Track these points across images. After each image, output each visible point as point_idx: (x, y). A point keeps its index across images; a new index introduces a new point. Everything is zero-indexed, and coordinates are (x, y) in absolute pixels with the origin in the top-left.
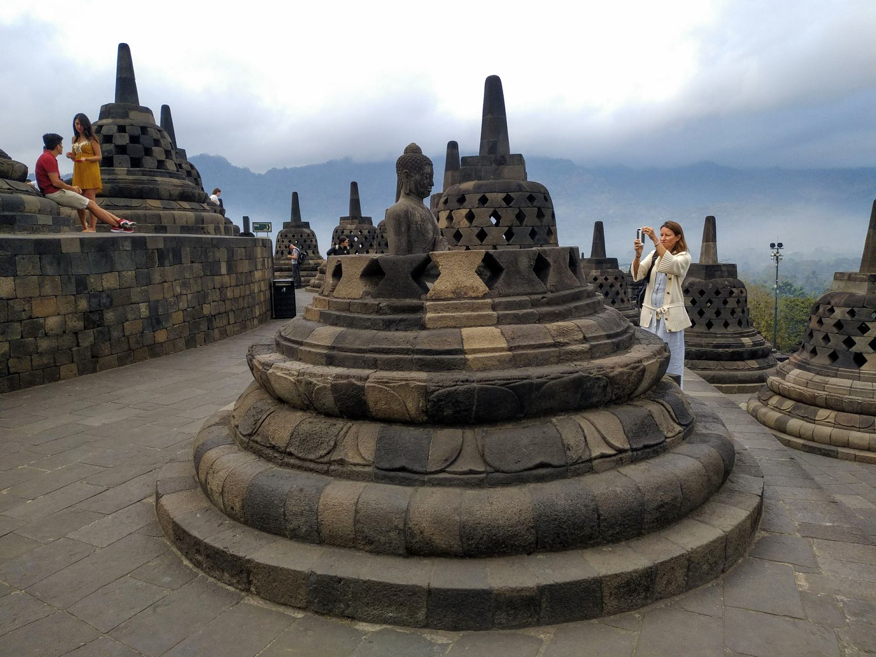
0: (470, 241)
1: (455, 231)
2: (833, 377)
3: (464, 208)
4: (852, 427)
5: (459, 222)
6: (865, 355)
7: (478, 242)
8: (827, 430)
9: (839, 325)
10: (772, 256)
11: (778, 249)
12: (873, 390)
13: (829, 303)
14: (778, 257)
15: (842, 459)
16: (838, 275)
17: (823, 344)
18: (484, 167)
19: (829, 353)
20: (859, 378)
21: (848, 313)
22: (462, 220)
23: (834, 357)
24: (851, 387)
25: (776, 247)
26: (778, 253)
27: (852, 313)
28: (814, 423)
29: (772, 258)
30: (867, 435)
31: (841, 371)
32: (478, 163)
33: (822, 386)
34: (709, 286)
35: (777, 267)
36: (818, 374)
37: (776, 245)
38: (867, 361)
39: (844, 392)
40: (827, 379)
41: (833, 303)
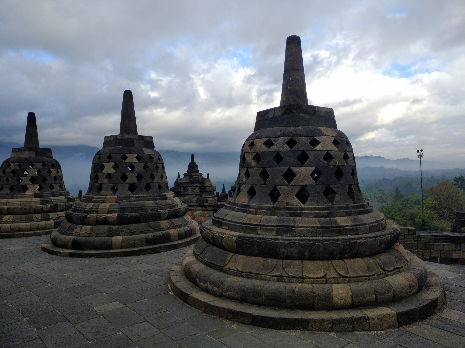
2: (11, 199)
4: (22, 221)
6: (27, 186)
8: (9, 225)
9: (14, 172)
12: (32, 201)
15: (17, 237)
16: (13, 149)
17: (6, 183)
19: (10, 187)
20: (25, 197)
21: (17, 165)
23: (12, 189)
24: (21, 202)
27: (20, 165)
28: (2, 224)
30: (29, 223)
31: (16, 195)
33: (5, 203)
36: (4, 198)
38: (29, 189)
39: (18, 205)
40: (8, 200)
41: (10, 161)
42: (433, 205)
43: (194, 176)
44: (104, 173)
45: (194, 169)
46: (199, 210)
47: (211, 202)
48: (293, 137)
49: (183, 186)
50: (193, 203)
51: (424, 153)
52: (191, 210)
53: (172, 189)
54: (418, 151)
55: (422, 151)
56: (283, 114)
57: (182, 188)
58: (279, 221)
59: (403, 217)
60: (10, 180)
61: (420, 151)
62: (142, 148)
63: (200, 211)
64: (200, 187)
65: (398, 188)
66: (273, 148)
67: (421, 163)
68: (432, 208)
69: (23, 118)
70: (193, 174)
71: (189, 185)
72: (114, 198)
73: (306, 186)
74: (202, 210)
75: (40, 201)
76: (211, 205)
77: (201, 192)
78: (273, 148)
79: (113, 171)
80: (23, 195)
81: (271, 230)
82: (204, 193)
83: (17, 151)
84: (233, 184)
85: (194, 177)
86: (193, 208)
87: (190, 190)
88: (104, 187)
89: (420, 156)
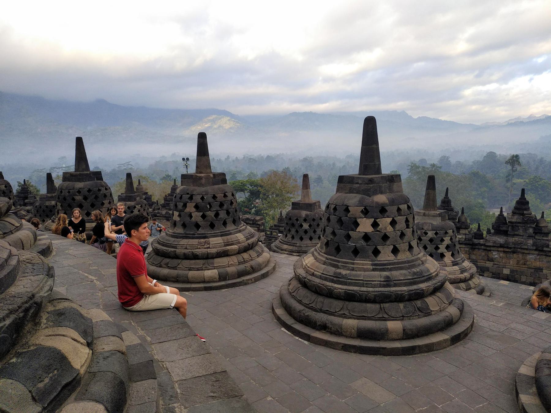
0: (396, 241)
1: (383, 234)
3: (388, 217)
6: (444, 254)
7: (317, 227)
9: (431, 240)
10: (184, 165)
11: (186, 161)
12: (454, 271)
13: (423, 229)
14: (186, 165)
21: (435, 234)
22: (388, 226)
25: (186, 160)
26: (187, 163)
29: (184, 166)
34: (316, 216)
35: (187, 171)
37: (185, 159)
41: (425, 228)
43: (527, 214)
45: (526, 206)
49: (512, 226)
50: (528, 246)
52: (524, 253)
53: (495, 226)
60: (428, 247)
63: (535, 255)
64: (534, 228)
70: (525, 212)
71: (521, 225)
74: (538, 255)
75: (460, 270)
77: (534, 233)
82: (538, 234)
83: (421, 215)
84: (412, 164)
85: (527, 215)
86: (526, 252)
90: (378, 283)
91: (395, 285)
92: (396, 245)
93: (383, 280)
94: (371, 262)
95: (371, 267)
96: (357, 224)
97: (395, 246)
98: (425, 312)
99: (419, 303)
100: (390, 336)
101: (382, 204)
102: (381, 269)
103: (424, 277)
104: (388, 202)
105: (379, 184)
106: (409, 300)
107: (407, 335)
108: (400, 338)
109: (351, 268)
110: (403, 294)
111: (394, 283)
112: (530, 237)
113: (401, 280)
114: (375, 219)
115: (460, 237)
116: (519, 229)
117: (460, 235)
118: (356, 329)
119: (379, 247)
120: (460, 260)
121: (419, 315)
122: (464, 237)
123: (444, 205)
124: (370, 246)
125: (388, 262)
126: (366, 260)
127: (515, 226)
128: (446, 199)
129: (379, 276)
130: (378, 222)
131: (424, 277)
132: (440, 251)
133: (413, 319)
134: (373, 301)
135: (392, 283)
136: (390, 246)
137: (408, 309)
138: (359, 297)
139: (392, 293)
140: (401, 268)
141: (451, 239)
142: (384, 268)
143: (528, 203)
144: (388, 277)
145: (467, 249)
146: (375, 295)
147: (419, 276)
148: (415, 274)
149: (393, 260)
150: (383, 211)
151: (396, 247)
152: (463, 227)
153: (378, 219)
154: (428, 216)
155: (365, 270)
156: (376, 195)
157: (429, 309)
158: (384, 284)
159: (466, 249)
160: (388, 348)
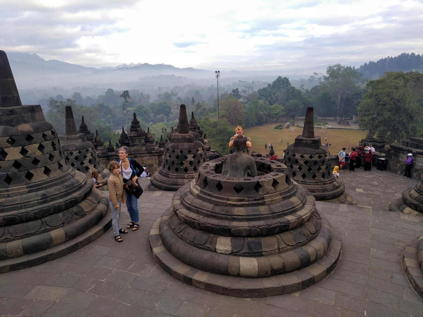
3: (35, 143)
5: (35, 153)
6: (88, 167)
9: (77, 158)
13: (68, 150)
18: (26, 115)
22: (36, 152)
32: (22, 112)
41: (70, 149)
42: (225, 114)
44: (187, 161)
45: (138, 125)
46: (147, 156)
47: (157, 150)
48: (320, 155)
51: (220, 74)
52: (141, 157)
54: (216, 72)
55: (219, 72)
56: (312, 143)
57: (130, 140)
58: (322, 187)
59: (210, 125)
60: (75, 164)
61: (217, 72)
62: (364, 192)
63: (148, 157)
64: (145, 140)
65: (193, 97)
66: (313, 159)
67: (218, 82)
68: (225, 116)
69: (81, 117)
70: (138, 129)
72: (197, 175)
73: (324, 173)
74: (149, 156)
75: (102, 176)
76: (157, 152)
77: (145, 142)
78: (313, 159)
79: (193, 159)
80: (89, 174)
81: (320, 191)
86: (142, 155)
87: (137, 141)
88: (189, 169)
89: (217, 76)
90: (35, 202)
91: (52, 200)
92: (47, 166)
93: (40, 198)
94: (26, 186)
95: (27, 190)
96: (5, 154)
97: (46, 167)
98: (80, 214)
99: (75, 209)
100: (55, 242)
101: (27, 132)
102: (36, 189)
103: (75, 187)
104: (32, 130)
105: (21, 115)
106: (66, 209)
107: (69, 237)
108: (64, 241)
109: (6, 195)
110: (60, 205)
111: (51, 198)
112: (143, 145)
113: (57, 194)
114: (23, 146)
115: (98, 152)
116: (136, 141)
117: (98, 151)
118: (21, 247)
119: (31, 171)
120: (101, 169)
121: (76, 218)
122: (101, 152)
123: (82, 130)
124: (21, 171)
125: (42, 182)
126: (20, 185)
127: (133, 139)
128: (83, 125)
129: (35, 196)
130: (26, 149)
131: (75, 187)
132: (85, 165)
133: (72, 223)
134: (34, 218)
135: (49, 199)
136: (42, 168)
137: (66, 216)
138: (19, 219)
139: (51, 207)
140: (55, 185)
141: (92, 155)
142: (39, 188)
143: (138, 122)
144: (44, 195)
145: (105, 160)
146: (35, 213)
147: (72, 188)
148: (67, 186)
149: (46, 179)
150: (29, 138)
151: (47, 168)
152: (99, 145)
153: (25, 146)
154: (71, 139)
155: (21, 194)
156: (19, 125)
157: (84, 211)
158: (41, 202)
159: (104, 161)
160: (55, 253)
